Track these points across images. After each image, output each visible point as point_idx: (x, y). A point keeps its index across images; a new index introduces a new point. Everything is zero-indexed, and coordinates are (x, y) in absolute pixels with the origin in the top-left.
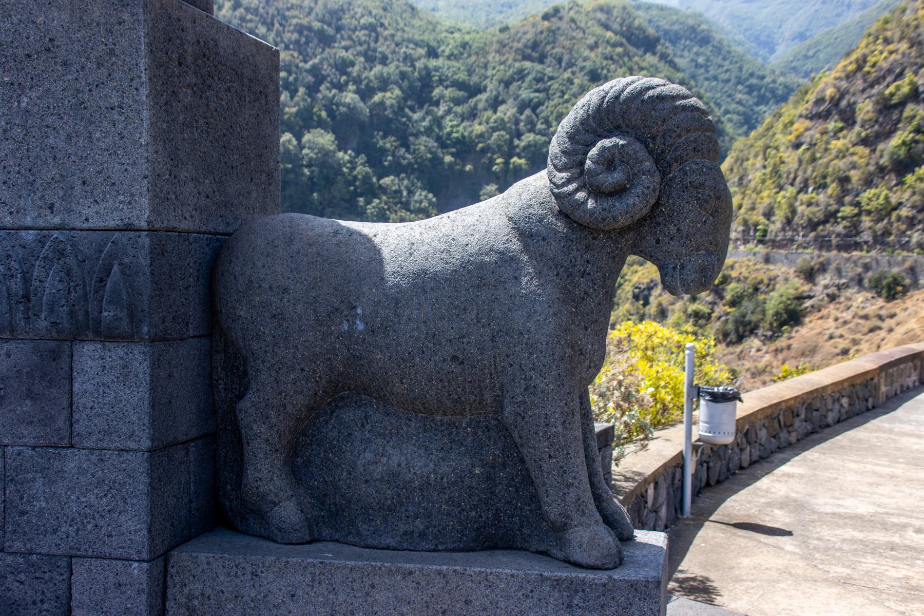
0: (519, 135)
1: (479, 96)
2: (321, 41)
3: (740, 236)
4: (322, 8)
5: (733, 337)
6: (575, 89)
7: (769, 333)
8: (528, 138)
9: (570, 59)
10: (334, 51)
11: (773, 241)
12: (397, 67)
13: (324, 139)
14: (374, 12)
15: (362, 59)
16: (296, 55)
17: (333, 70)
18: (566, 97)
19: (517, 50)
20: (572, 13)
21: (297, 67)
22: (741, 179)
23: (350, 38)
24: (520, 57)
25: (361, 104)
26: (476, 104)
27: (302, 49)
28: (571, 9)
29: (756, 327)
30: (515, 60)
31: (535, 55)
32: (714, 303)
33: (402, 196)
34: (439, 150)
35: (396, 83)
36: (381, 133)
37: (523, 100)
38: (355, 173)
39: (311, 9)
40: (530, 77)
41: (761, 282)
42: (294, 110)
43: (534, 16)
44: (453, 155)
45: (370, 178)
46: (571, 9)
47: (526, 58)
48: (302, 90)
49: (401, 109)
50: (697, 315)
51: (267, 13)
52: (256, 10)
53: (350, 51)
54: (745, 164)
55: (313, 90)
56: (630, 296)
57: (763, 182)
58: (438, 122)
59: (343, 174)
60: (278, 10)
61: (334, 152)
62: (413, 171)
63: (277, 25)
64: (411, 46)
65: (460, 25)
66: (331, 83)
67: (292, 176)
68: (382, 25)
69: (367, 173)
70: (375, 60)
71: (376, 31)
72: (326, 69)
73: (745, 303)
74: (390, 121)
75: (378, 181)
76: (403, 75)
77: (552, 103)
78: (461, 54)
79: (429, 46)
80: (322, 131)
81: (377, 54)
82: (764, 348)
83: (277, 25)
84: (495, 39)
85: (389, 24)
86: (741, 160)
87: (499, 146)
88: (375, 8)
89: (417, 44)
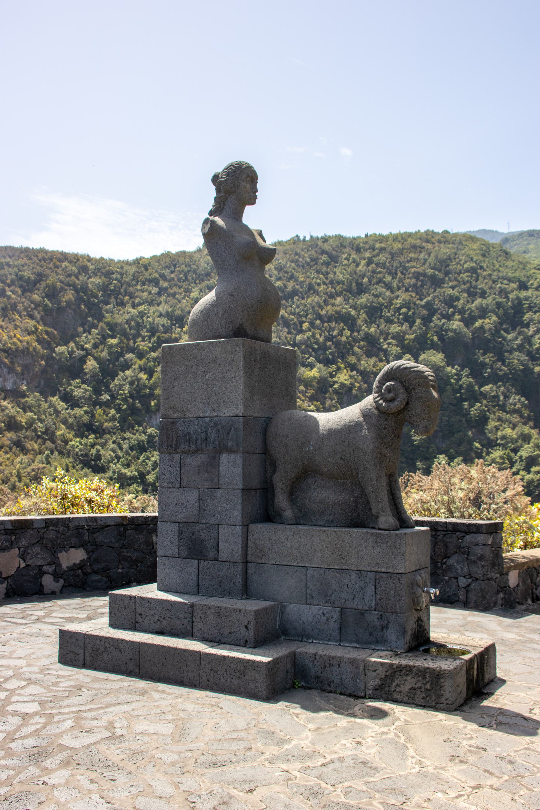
2: (433, 284)
4: (434, 258)
10: (444, 290)
12: (494, 299)
13: (438, 358)
14: (475, 258)
15: (466, 295)
16: (414, 295)
17: (443, 305)
21: (415, 304)
23: (456, 279)
25: (465, 329)
27: (418, 290)
33: (499, 400)
34: (530, 363)
35: (493, 311)
36: (481, 351)
38: (461, 383)
39: (426, 260)
42: (412, 337)
45: (473, 387)
49: (497, 331)
51: (392, 266)
53: (455, 290)
55: (427, 320)
58: (528, 340)
59: (451, 384)
60: (400, 263)
61: (444, 367)
62: (508, 380)
63: (399, 274)
64: (505, 282)
66: (441, 314)
68: (482, 268)
69: (470, 383)
70: (476, 295)
71: (476, 273)
74: (489, 341)
75: (479, 389)
76: (499, 305)
79: (520, 281)
80: (435, 352)
81: (478, 290)
83: (399, 274)
85: (487, 267)
88: (476, 255)
89: (510, 280)
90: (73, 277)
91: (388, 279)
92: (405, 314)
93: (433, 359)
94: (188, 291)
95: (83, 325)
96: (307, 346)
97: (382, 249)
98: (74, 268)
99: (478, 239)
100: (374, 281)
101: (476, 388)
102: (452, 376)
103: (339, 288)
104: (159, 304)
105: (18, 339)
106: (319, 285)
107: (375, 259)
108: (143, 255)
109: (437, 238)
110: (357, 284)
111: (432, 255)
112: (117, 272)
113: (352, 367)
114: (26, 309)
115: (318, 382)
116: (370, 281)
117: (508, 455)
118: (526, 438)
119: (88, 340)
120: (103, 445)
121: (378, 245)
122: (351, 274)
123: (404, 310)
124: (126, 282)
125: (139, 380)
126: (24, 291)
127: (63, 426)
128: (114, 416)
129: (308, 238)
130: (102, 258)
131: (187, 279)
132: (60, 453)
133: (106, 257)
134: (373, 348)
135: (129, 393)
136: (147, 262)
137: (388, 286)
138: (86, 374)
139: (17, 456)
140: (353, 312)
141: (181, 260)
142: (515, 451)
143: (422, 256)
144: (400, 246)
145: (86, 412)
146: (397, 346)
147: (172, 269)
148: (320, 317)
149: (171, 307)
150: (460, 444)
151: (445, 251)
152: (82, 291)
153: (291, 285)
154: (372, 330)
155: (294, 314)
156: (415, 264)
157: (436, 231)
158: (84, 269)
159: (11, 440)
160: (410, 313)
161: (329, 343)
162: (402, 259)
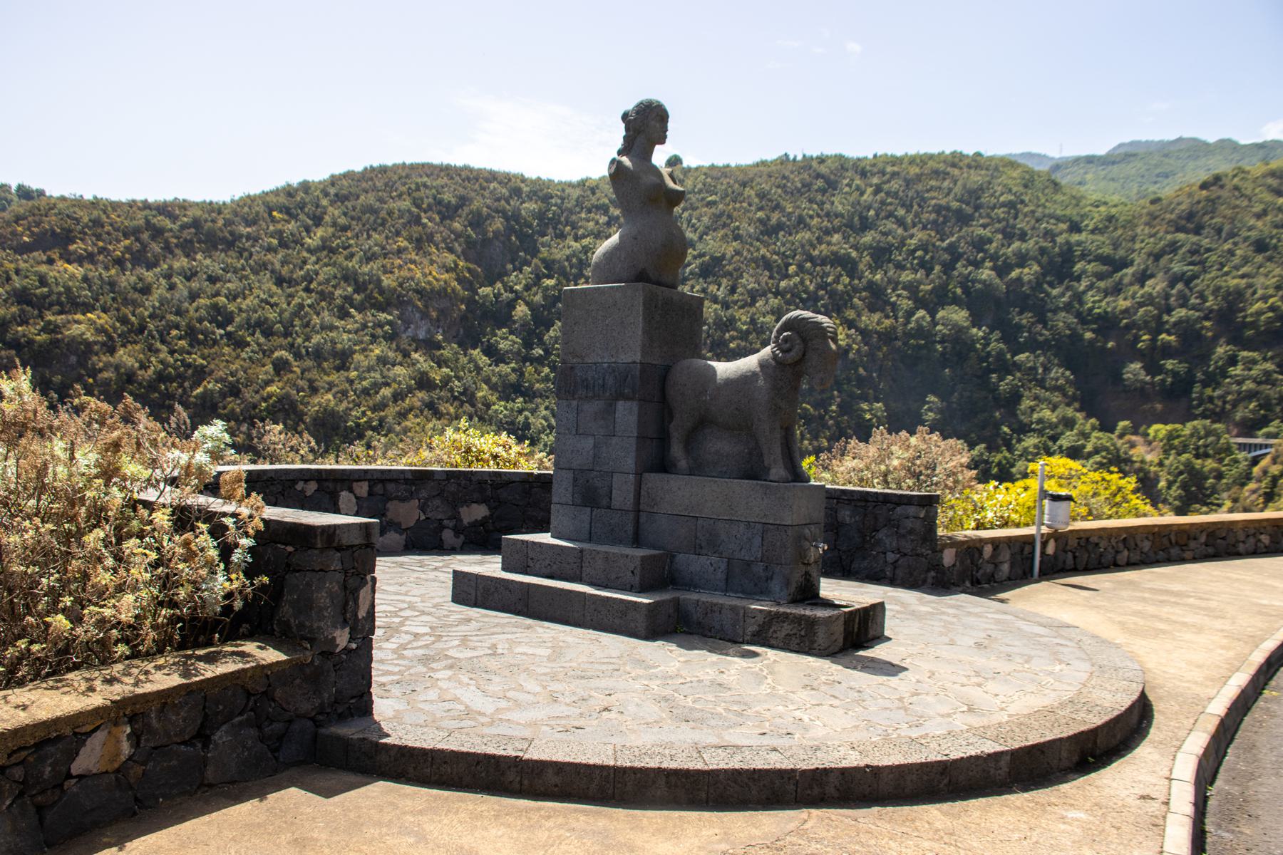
0: (1169, 311)
1: (1125, 271)
2: (958, 220)
6: (1236, 260)
8: (1181, 313)
9: (1232, 229)
12: (1037, 243)
13: (959, 316)
14: (1015, 189)
15: (1000, 236)
16: (933, 234)
18: (1226, 269)
19: (1170, 221)
20: (1236, 180)
21: (934, 245)
23: (988, 216)
24: (1172, 229)
25: (998, 281)
26: (1121, 279)
28: (1235, 176)
30: (1167, 232)
31: (1190, 226)
33: (1037, 373)
34: (1079, 327)
35: (1035, 259)
37: (1175, 273)
39: (950, 190)
40: (1184, 249)
42: (929, 287)
43: (1190, 186)
44: (1093, 331)
46: (1235, 176)
47: (1178, 230)
48: (937, 268)
52: (897, 193)
55: (948, 267)
58: (1079, 297)
59: (976, 350)
60: (917, 192)
62: (1050, 347)
63: (916, 207)
64: (1052, 221)
65: (1108, 199)
66: (968, 260)
67: (925, 352)
68: (1022, 202)
71: (1015, 208)
72: (963, 247)
74: (1027, 297)
76: (1043, 251)
77: (1208, 276)
78: (1107, 227)
79: (1070, 220)
83: (916, 207)
84: (1145, 211)
87: (1146, 322)
88: (1015, 185)
89: (1059, 219)
91: (901, 212)
92: (921, 259)
93: (955, 317)
95: (512, 262)
96: (792, 295)
97: (894, 175)
99: (1019, 165)
100: (883, 214)
101: (1009, 356)
102: (978, 340)
103: (837, 222)
105: (434, 278)
106: (811, 217)
107: (886, 187)
109: (966, 161)
110: (861, 218)
111: (959, 183)
114: (444, 240)
116: (877, 215)
118: (1069, 423)
119: (518, 281)
120: (533, 412)
121: (889, 169)
122: (853, 205)
123: (919, 253)
124: (567, 209)
126: (442, 219)
127: (485, 386)
128: (547, 375)
129: (799, 158)
130: (539, 179)
132: (481, 419)
133: (544, 177)
134: (877, 299)
137: (901, 222)
138: (515, 322)
139: (429, 421)
140: (854, 254)
142: (1054, 438)
143: (946, 184)
144: (917, 170)
145: (514, 370)
146: (909, 299)
148: (811, 259)
150: (984, 428)
151: (976, 178)
152: (513, 218)
153: (775, 217)
154: (878, 277)
155: (778, 254)
156: (935, 194)
157: (965, 152)
158: (517, 192)
159: (422, 400)
161: (822, 293)
162: (920, 187)
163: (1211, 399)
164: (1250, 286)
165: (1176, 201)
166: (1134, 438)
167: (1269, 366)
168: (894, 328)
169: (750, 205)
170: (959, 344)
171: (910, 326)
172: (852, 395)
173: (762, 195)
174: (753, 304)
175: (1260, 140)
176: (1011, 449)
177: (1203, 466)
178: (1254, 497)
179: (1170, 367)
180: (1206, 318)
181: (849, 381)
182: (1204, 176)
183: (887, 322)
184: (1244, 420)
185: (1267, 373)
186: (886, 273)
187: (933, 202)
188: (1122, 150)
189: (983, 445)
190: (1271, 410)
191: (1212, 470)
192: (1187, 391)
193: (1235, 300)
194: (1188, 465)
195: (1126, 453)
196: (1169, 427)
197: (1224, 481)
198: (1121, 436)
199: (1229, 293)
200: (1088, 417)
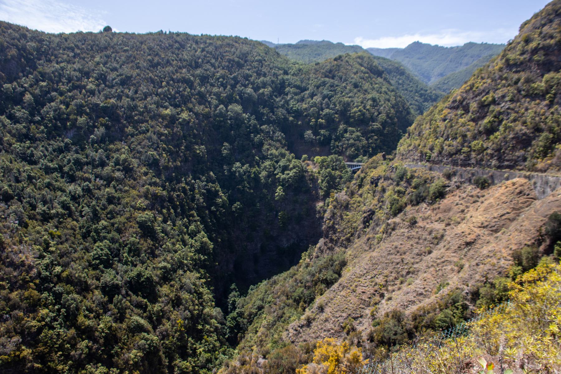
1: (305, 92)
2: (238, 66)
3: (419, 158)
5: (415, 202)
6: (347, 91)
7: (431, 201)
8: (327, 111)
10: (243, 70)
11: (433, 161)
13: (238, 108)
14: (261, 54)
15: (255, 74)
20: (346, 58)
21: (227, 77)
22: (420, 133)
23: (251, 65)
25: (254, 93)
26: (304, 95)
29: (425, 198)
30: (322, 77)
31: (330, 75)
32: (406, 187)
35: (270, 85)
39: (234, 53)
40: (328, 85)
41: (428, 178)
42: (225, 95)
44: (293, 117)
45: (256, 126)
47: (326, 76)
49: (271, 96)
50: (399, 192)
52: (211, 52)
54: (422, 127)
55: (233, 87)
56: (369, 182)
57: (430, 135)
58: (287, 102)
59: (245, 123)
60: (220, 53)
61: (241, 114)
62: (275, 123)
63: (219, 59)
64: (277, 69)
65: (297, 62)
66: (242, 84)
67: (223, 123)
68: (265, 60)
71: (262, 63)
72: (240, 78)
73: (420, 188)
74: (266, 101)
76: (273, 82)
77: (337, 96)
78: (298, 74)
79: (284, 70)
82: (428, 208)
83: (219, 59)
86: (420, 125)
87: (313, 114)
88: (262, 53)
89: (279, 69)
90: (16, 41)
91: (213, 61)
92: (222, 82)
93: (236, 108)
94: (93, 57)
95: (23, 72)
96: (164, 96)
97: (210, 44)
98: (16, 35)
100: (205, 61)
102: (246, 119)
103: (184, 63)
104: (74, 63)
106: (173, 60)
107: (207, 49)
108: (64, 32)
109: (241, 41)
110: (195, 62)
111: (238, 50)
112: (46, 40)
113: (190, 110)
115: (170, 118)
116: (203, 62)
117: (273, 164)
118: (283, 156)
119: (26, 81)
120: (36, 148)
121: (208, 41)
122: (192, 56)
123: (221, 80)
124: (52, 47)
125: (60, 109)
127: (8, 135)
128: (43, 130)
129: (168, 33)
130: (36, 31)
131: (92, 49)
132: (6, 151)
133: (39, 30)
134: (202, 99)
135: (53, 116)
136: (67, 36)
137: (213, 65)
138: (24, 103)
141: (89, 37)
142: (277, 162)
143: (233, 50)
144: (220, 43)
145: (24, 127)
146: (216, 100)
147: (83, 42)
148: (173, 79)
149: (82, 65)
150: (248, 157)
151: (246, 48)
152: (22, 50)
153: (156, 59)
154: (203, 89)
155: (157, 76)
156: (228, 54)
157: (241, 37)
158: (24, 36)
160: (224, 82)
161: (177, 95)
163: (338, 146)
164: (352, 101)
165: (325, 65)
166: (308, 162)
167: (359, 134)
168: (209, 112)
169: (144, 53)
170: (238, 121)
171: (216, 112)
172: (191, 142)
173: (150, 49)
174: (146, 99)
175: (352, 44)
176: (259, 166)
177: (335, 174)
178: (355, 186)
179: (322, 133)
180: (336, 113)
181: (190, 135)
182: (337, 55)
183: (207, 110)
184: (350, 155)
185: (358, 137)
186: (206, 88)
187: (227, 57)
188: (302, 43)
189: (248, 165)
190: (359, 151)
191: (339, 175)
192: (329, 143)
193: (347, 106)
194: (330, 174)
195: (306, 168)
196: (322, 158)
197: (343, 180)
198: (303, 161)
199: (345, 104)
200: (291, 153)
